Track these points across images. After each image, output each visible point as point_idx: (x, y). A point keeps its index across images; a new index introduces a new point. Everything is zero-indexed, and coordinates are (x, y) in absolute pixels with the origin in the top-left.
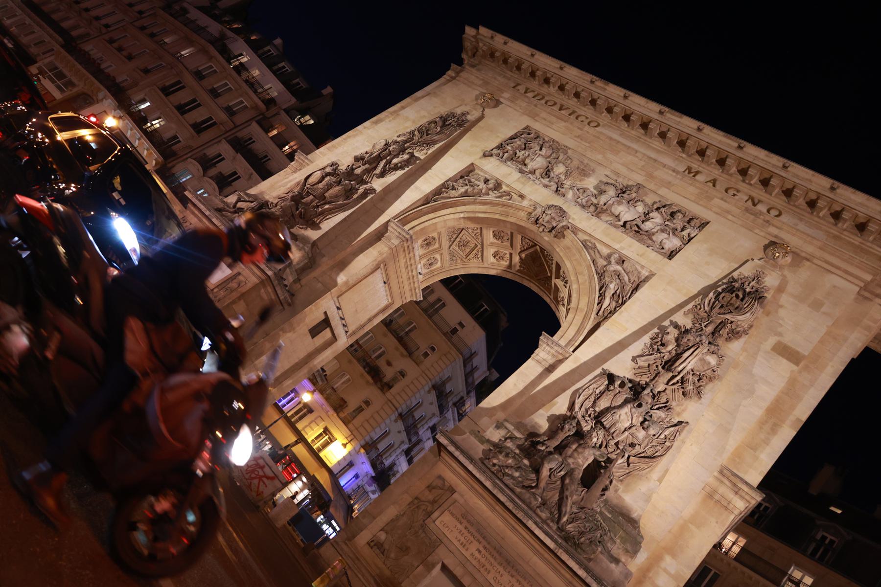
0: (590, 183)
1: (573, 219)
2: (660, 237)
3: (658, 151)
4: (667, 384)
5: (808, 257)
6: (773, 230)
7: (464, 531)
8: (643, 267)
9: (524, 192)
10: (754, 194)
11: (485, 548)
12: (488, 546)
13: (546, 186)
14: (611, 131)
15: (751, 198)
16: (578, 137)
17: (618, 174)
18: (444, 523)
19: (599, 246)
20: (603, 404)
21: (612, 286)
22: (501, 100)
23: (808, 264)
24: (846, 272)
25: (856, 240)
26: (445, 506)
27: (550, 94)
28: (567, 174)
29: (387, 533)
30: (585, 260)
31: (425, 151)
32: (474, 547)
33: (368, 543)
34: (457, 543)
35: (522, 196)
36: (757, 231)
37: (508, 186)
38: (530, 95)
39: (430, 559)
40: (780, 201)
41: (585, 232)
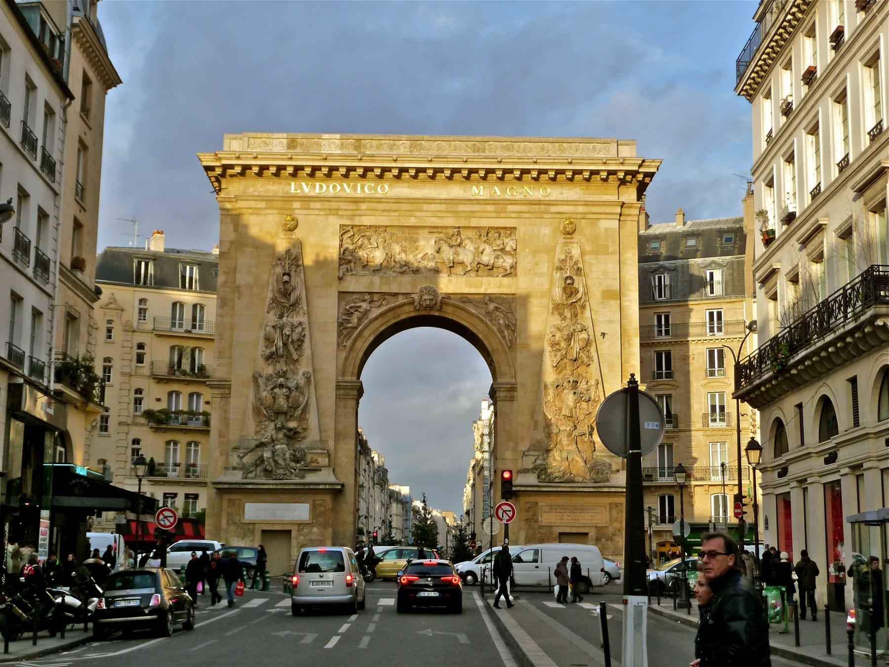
13: (402, 273)
21: (501, 322)
31: (301, 311)
32: (565, 516)
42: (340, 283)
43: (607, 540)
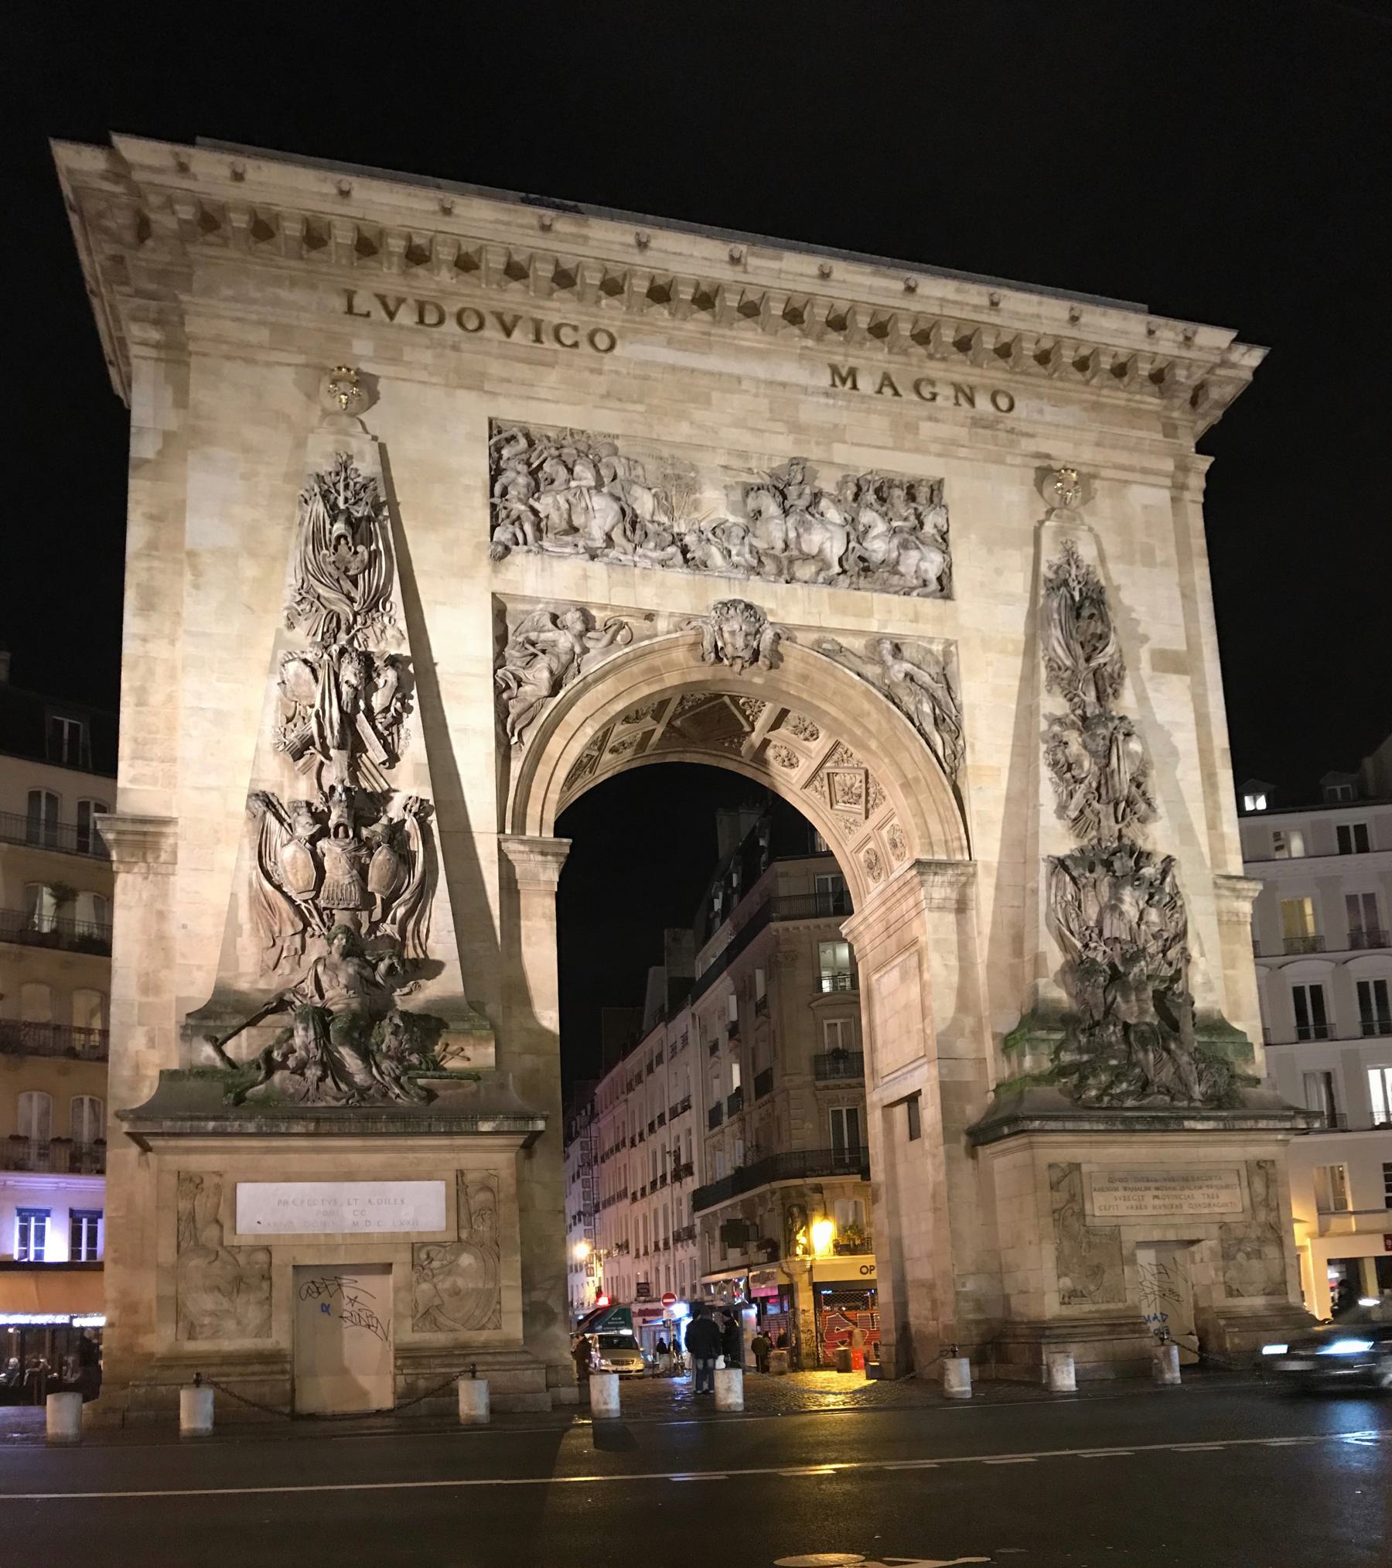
0: (715, 504)
1: (771, 611)
2: (911, 561)
3: (761, 354)
4: (1117, 822)
5: (1091, 470)
6: (1028, 445)
7: (1127, 1193)
8: (931, 640)
9: (649, 605)
10: (957, 378)
11: (1157, 1189)
12: (1158, 1184)
13: (664, 564)
14: (652, 348)
15: (958, 388)
16: (608, 396)
17: (744, 455)
18: (1103, 1206)
19: (844, 641)
20: (1092, 912)
22: (367, 367)
23: (1097, 484)
24: (1144, 471)
25: (1120, 398)
26: (1086, 1190)
27: (445, 293)
28: (664, 503)
29: (1066, 1275)
30: (853, 686)
33: (1063, 1303)
34: (1133, 1212)
35: (650, 616)
36: (1009, 459)
37: (603, 607)
38: (406, 317)
39: (1125, 1252)
40: (995, 374)
41: (809, 628)
42: (495, 571)
43: (1248, 1255)
